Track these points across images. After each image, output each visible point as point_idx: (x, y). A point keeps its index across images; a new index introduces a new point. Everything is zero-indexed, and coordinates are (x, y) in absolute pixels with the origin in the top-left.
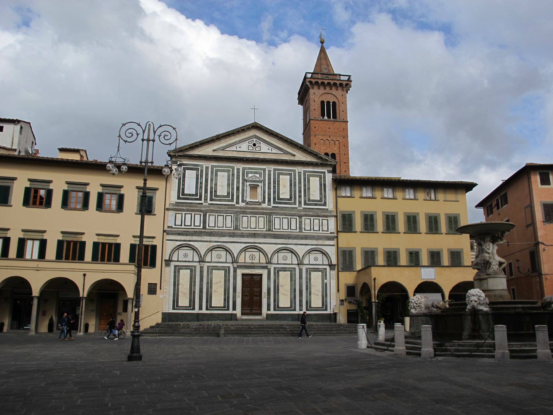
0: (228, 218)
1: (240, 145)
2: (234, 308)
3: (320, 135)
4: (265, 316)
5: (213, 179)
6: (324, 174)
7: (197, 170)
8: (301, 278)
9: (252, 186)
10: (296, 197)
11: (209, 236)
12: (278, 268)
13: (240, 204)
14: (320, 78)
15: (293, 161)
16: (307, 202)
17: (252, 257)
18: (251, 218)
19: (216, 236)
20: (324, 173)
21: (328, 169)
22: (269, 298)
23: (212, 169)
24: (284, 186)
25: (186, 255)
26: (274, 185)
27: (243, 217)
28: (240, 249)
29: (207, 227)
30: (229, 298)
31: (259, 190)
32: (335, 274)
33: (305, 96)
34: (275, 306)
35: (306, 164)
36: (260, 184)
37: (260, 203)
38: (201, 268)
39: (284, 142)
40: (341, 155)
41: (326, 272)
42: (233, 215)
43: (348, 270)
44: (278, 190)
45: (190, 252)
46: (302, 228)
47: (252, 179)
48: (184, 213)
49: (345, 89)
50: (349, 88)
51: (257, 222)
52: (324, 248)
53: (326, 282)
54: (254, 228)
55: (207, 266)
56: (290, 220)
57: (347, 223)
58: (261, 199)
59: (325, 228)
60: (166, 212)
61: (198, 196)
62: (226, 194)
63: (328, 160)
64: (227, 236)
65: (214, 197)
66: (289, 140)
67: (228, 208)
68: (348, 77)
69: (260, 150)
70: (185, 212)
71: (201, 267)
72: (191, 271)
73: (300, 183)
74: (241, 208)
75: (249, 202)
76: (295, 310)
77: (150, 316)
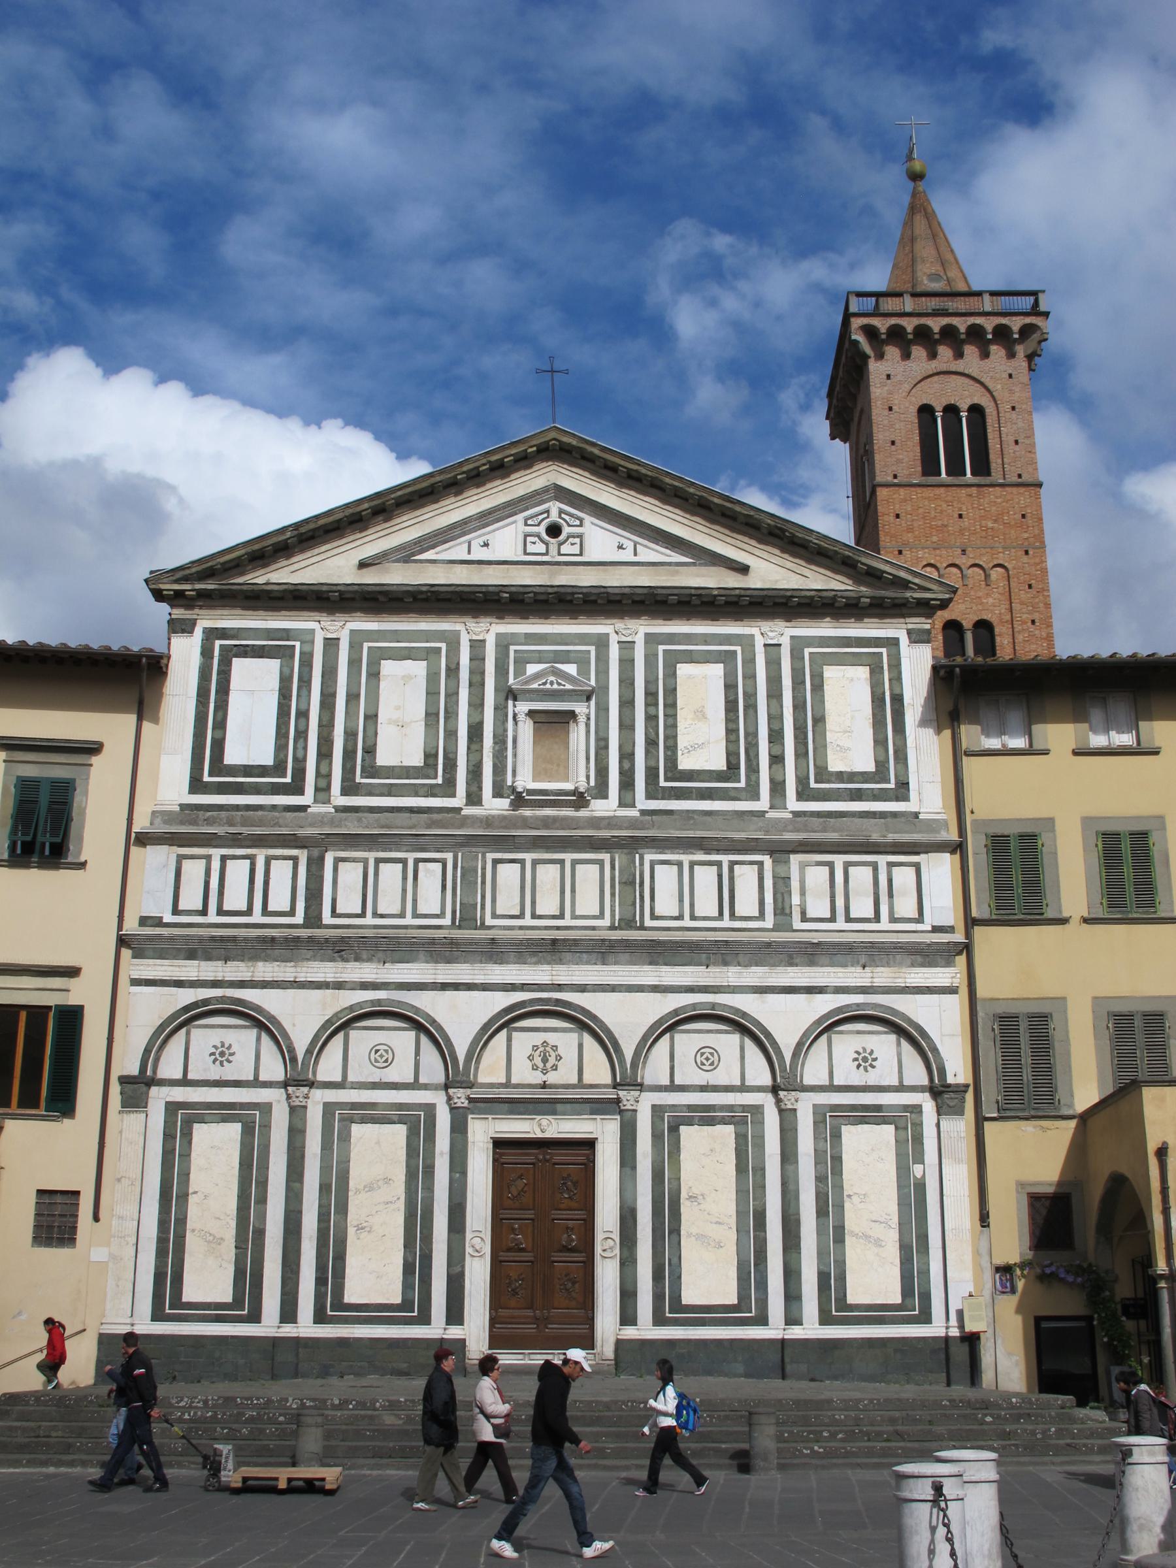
0: (427, 871)
1: (484, 534)
2: (455, 1315)
3: (923, 548)
4: (609, 1352)
5: (358, 696)
6: (893, 650)
7: (284, 654)
8: (788, 1155)
9: (542, 718)
10: (758, 764)
11: (332, 960)
12: (673, 1107)
13: (486, 807)
14: (908, 309)
15: (737, 592)
16: (813, 785)
17: (545, 1057)
18: (540, 868)
19: (369, 960)
20: (894, 643)
21: (910, 626)
22: (628, 1262)
23: (355, 646)
24: (701, 714)
25: (222, 1055)
26: (652, 710)
27: (499, 866)
28: (485, 1020)
29: (327, 918)
30: (427, 1259)
31: (578, 736)
32: (963, 1135)
33: (854, 397)
34: (658, 1298)
35: (800, 605)
36: (580, 708)
37: (581, 795)
38: (297, 1113)
39: (693, 514)
40: (1018, 627)
41: (917, 1126)
42: (449, 857)
43: (1033, 1113)
44: (669, 732)
45: (243, 1040)
46: (787, 911)
47: (544, 684)
48: (216, 853)
49: (1020, 350)
50: (1040, 342)
51: (567, 889)
52: (902, 1004)
53: (919, 1175)
54: (554, 917)
55: (326, 1105)
56: (731, 870)
57: (1017, 878)
58: (588, 777)
59: (906, 906)
60: (134, 850)
61: (285, 776)
62: (417, 760)
63: (910, 582)
64: (421, 955)
65: (362, 777)
66: (716, 500)
67: (429, 827)
68: (1032, 299)
69: (581, 554)
70: (225, 851)
71: (293, 1110)
72: (248, 1131)
73: (775, 694)
74: (488, 822)
75: (531, 792)
76: (762, 1320)
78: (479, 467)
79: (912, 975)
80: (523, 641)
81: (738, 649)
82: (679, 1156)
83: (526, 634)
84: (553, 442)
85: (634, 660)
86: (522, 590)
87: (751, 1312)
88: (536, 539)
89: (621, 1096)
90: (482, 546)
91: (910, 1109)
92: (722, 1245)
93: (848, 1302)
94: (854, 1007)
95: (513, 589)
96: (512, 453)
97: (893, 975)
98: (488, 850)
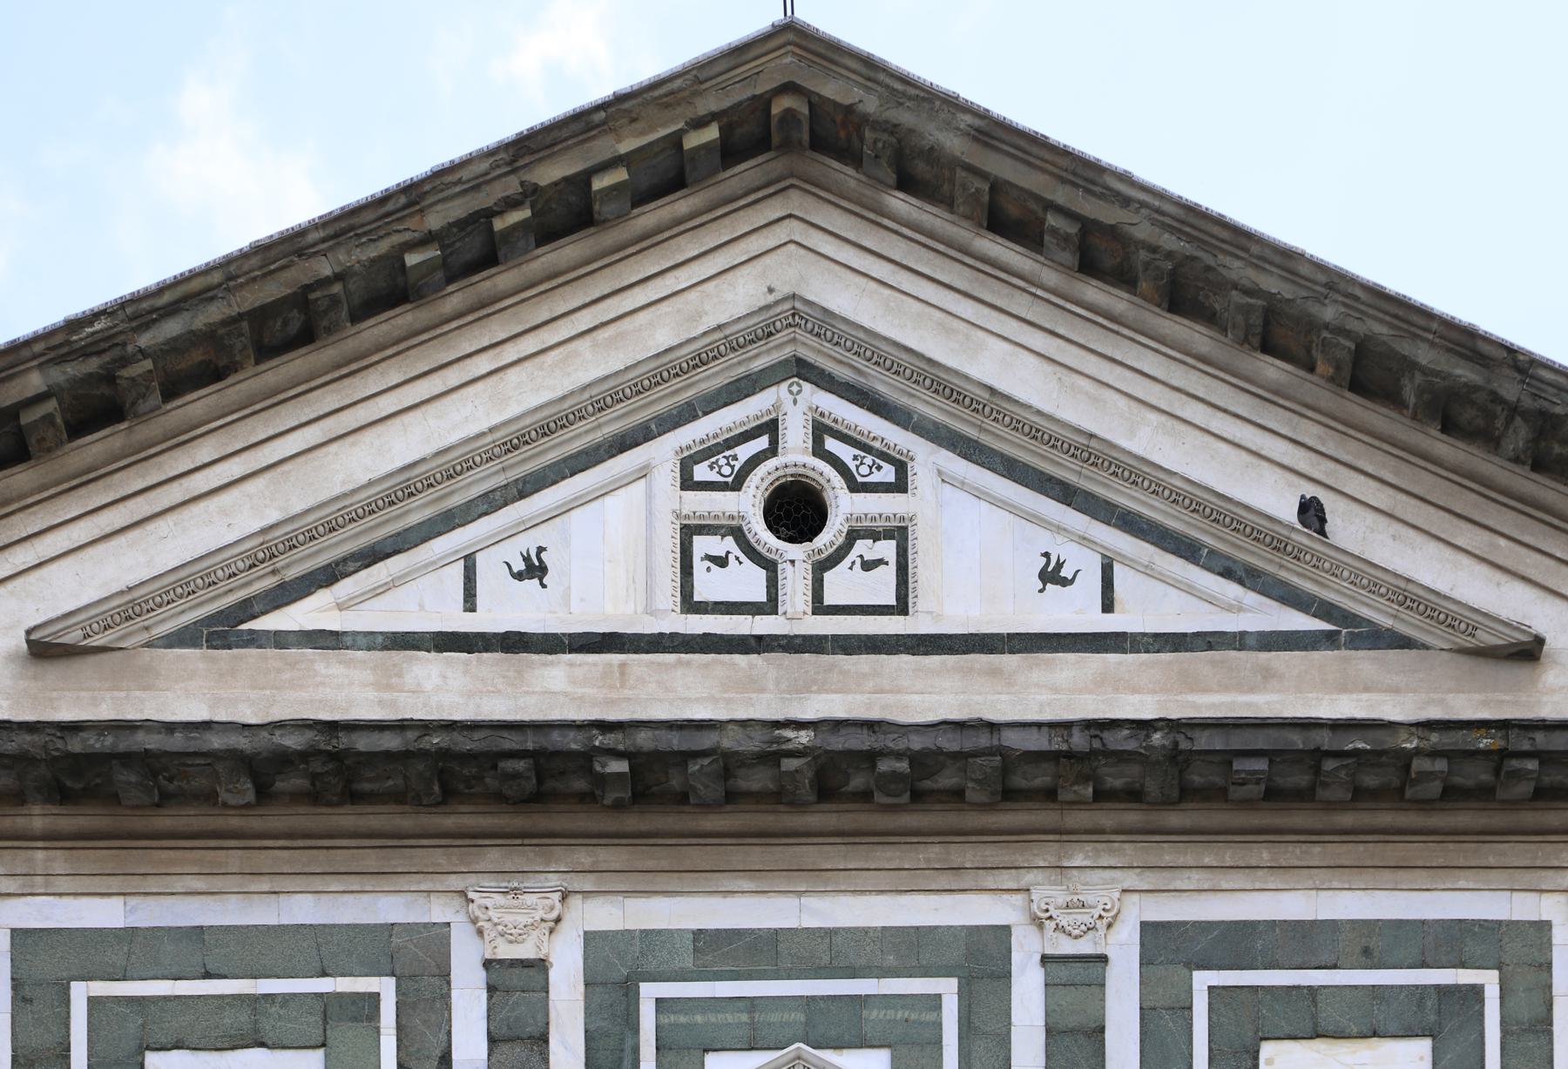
69: (901, 607)
80: (689, 962)
81: (1489, 980)
83: (697, 934)
85: (1102, 1030)
86: (676, 741)
88: (729, 544)
90: (519, 576)
95: (643, 739)
96: (625, 147)
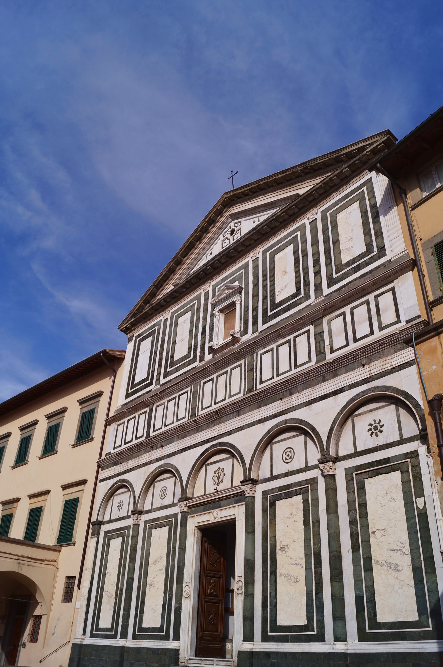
24: (285, 272)
41: (417, 467)
46: (322, 351)
53: (421, 507)
58: (241, 328)
77: (56, 651)
78: (203, 226)
79: (395, 359)
82: (276, 521)
84: (226, 199)
87: (314, 631)
89: (244, 489)
91: (410, 456)
92: (298, 580)
93: (378, 621)
94: (362, 394)
97: (382, 363)
98: (202, 379)
